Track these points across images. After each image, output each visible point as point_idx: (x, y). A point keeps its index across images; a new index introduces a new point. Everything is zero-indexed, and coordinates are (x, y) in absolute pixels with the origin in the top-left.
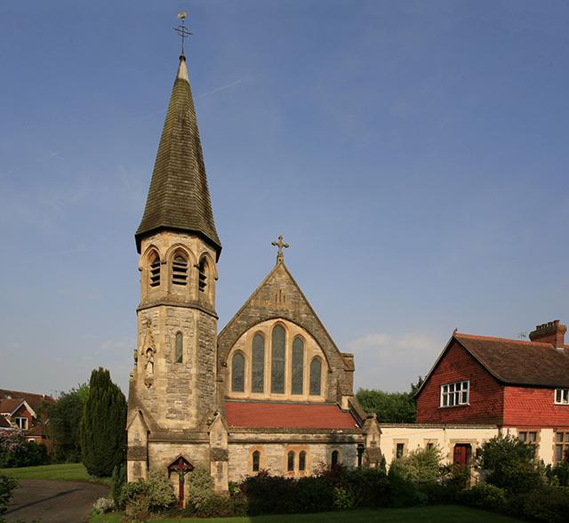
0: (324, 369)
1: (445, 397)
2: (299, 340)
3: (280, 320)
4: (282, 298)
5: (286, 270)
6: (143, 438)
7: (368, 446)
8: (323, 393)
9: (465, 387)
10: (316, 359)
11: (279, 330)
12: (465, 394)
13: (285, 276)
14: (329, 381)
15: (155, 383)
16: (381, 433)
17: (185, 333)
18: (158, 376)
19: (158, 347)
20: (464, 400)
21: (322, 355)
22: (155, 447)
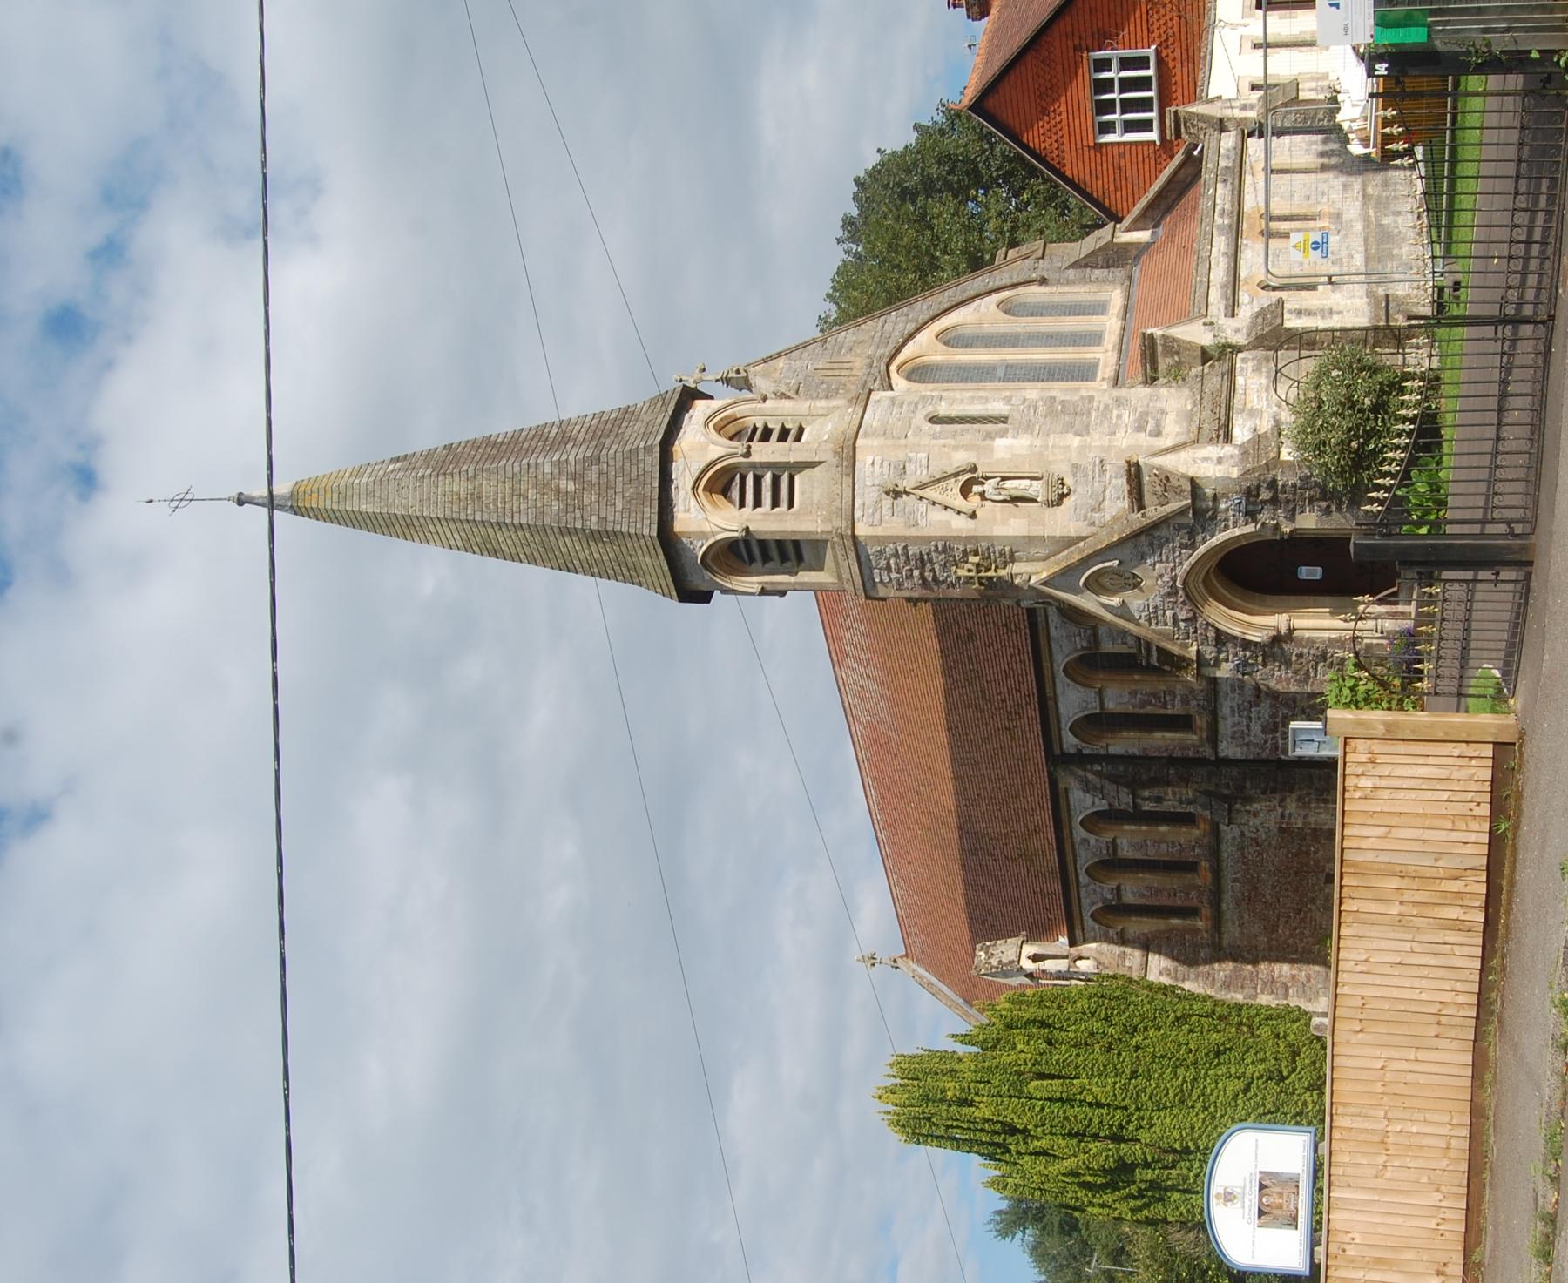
0: (1035, 293)
1: (1130, 127)
2: (949, 339)
3: (893, 368)
4: (836, 366)
5: (765, 361)
6: (1213, 451)
7: (1252, 114)
8: (1101, 297)
9: (1104, 65)
10: (1008, 308)
11: (919, 373)
12: (1126, 63)
13: (781, 363)
14: (1069, 282)
15: (1062, 469)
16: (1219, 98)
17: (930, 409)
18: (1041, 454)
19: (961, 459)
20: (1143, 62)
21: (996, 297)
22: (1241, 433)
